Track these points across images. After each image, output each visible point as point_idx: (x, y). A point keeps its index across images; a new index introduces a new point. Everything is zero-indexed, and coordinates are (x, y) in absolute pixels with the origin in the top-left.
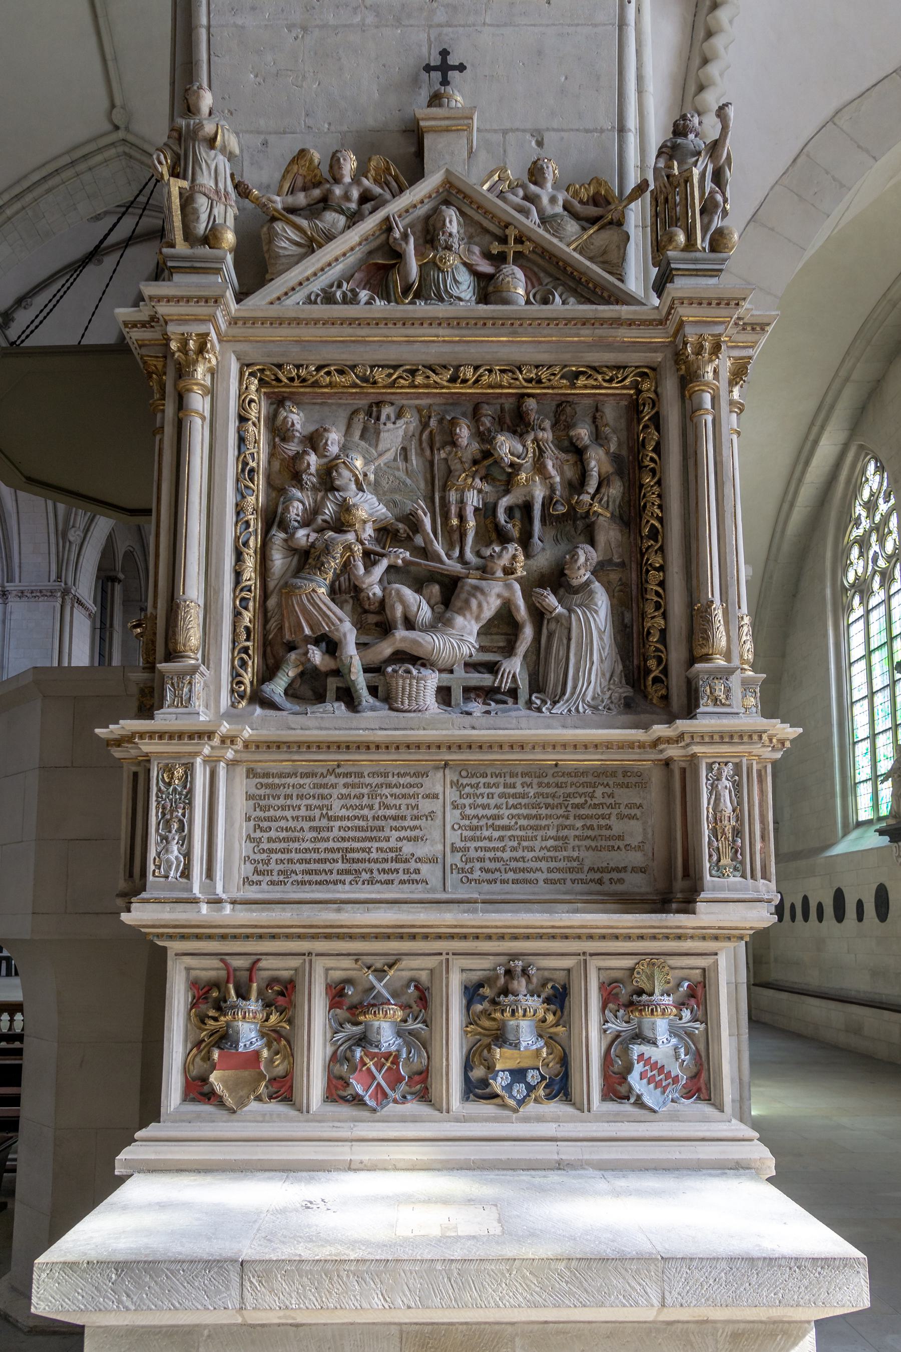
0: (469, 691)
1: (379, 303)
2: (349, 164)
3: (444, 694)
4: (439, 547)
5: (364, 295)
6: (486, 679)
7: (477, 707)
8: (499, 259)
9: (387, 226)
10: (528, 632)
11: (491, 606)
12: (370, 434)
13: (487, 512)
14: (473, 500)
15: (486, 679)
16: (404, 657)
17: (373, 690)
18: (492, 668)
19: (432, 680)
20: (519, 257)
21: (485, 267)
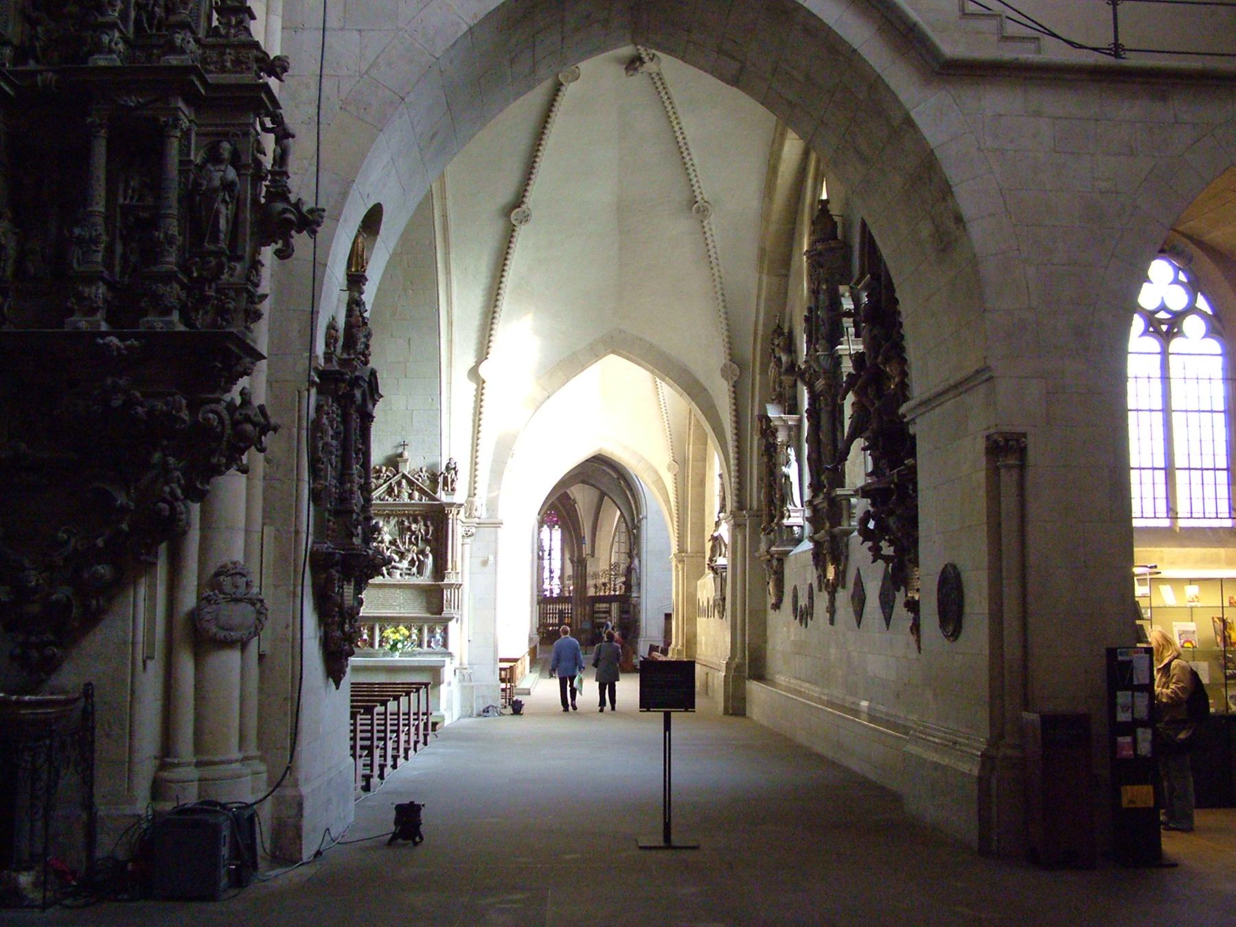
0: (406, 574)
1: (390, 499)
2: (384, 469)
3: (401, 575)
4: (401, 546)
5: (387, 497)
6: (408, 572)
7: (407, 577)
8: (413, 490)
9: (391, 484)
10: (417, 563)
11: (410, 559)
12: (388, 522)
13: (410, 539)
14: (407, 537)
15: (408, 572)
16: (394, 567)
17: (388, 574)
18: (410, 569)
19: (399, 572)
20: (417, 490)
21: (410, 492)
